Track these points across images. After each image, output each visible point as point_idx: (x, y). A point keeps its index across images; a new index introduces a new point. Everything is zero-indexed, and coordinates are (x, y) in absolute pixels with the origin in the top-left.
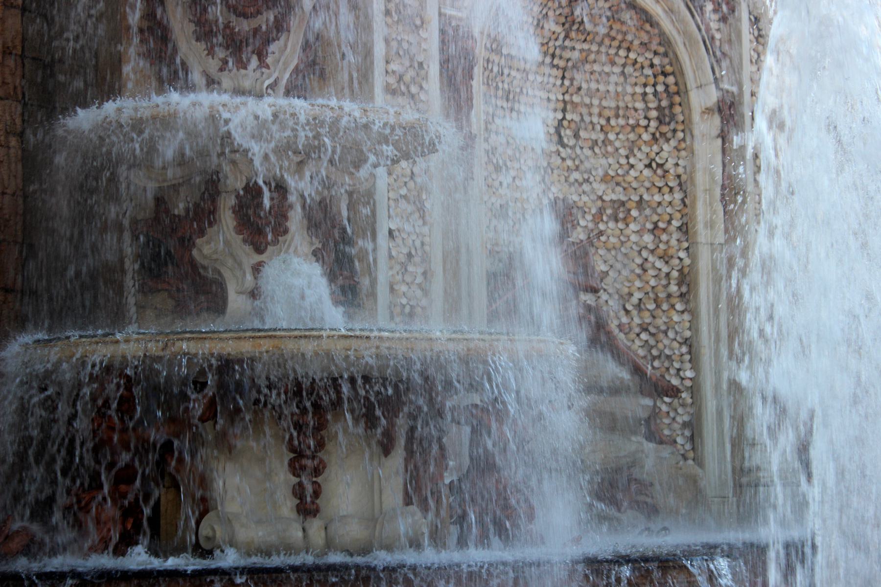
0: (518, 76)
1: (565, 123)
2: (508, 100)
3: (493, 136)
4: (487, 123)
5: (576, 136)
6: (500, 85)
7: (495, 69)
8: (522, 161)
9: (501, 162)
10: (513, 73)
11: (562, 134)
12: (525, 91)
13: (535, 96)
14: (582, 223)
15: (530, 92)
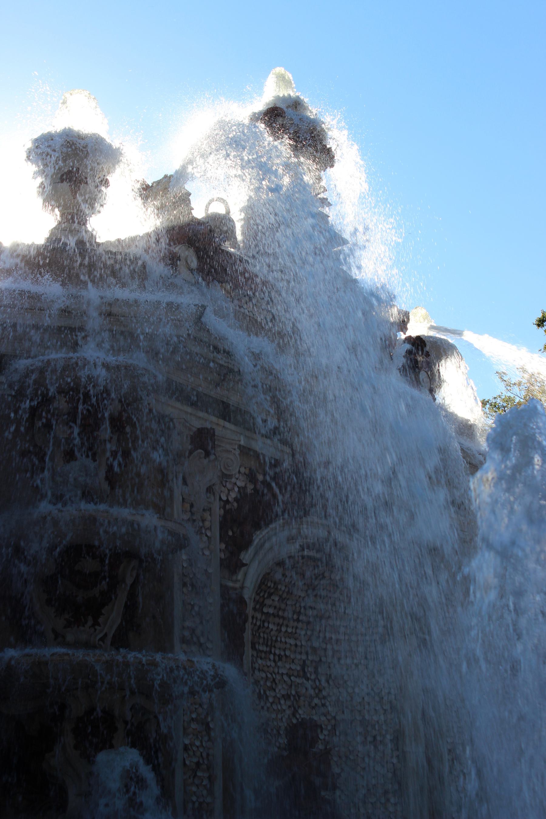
0: (275, 628)
1: (308, 663)
2: (267, 646)
3: (257, 672)
4: (253, 662)
5: (316, 672)
6: (262, 635)
7: (258, 623)
8: (277, 691)
9: (262, 692)
10: (271, 626)
11: (306, 670)
12: (279, 639)
13: (286, 643)
14: (321, 737)
15: (283, 640)
